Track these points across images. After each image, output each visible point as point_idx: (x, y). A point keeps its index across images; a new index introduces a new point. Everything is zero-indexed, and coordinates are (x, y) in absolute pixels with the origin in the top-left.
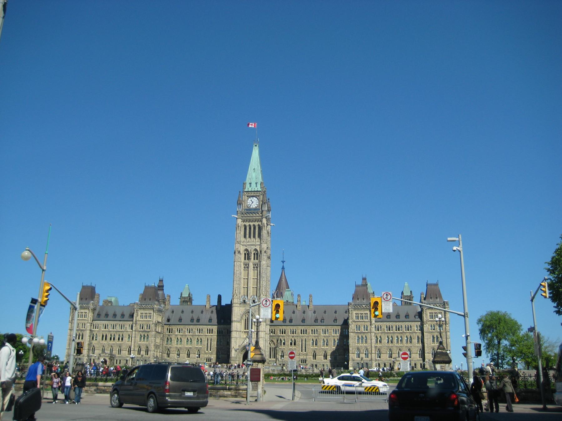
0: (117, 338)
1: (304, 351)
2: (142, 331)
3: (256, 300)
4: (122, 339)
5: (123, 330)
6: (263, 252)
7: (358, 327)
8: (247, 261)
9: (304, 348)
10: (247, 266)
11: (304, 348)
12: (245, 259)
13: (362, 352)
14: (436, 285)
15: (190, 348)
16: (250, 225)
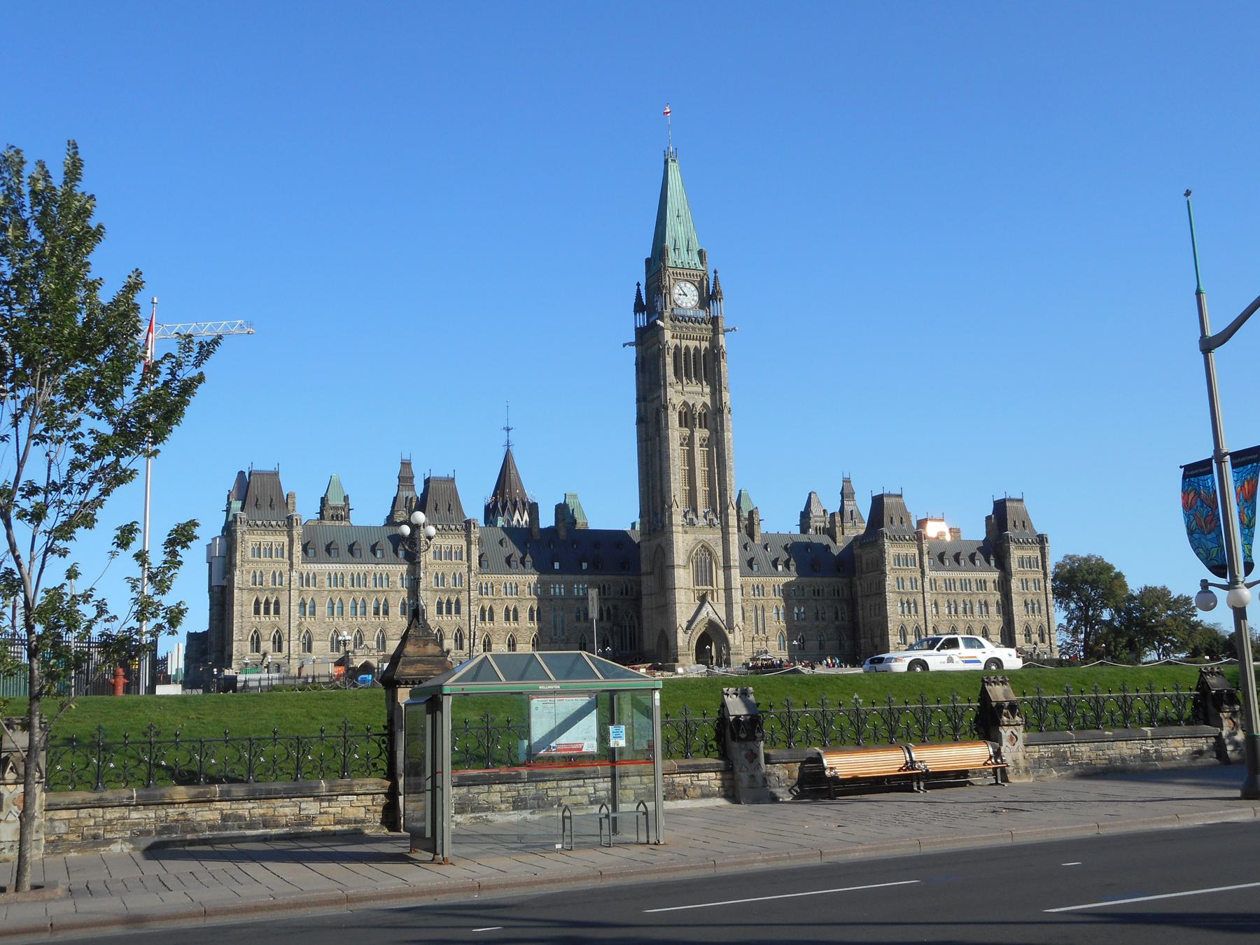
0: (371, 609)
1: (761, 632)
2: (442, 591)
3: (716, 521)
4: (386, 613)
5: (385, 588)
6: (726, 411)
7: (900, 581)
8: (686, 431)
9: (760, 626)
10: (689, 442)
11: (760, 626)
12: (681, 425)
13: (909, 631)
14: (1021, 500)
15: (516, 630)
16: (687, 348)
